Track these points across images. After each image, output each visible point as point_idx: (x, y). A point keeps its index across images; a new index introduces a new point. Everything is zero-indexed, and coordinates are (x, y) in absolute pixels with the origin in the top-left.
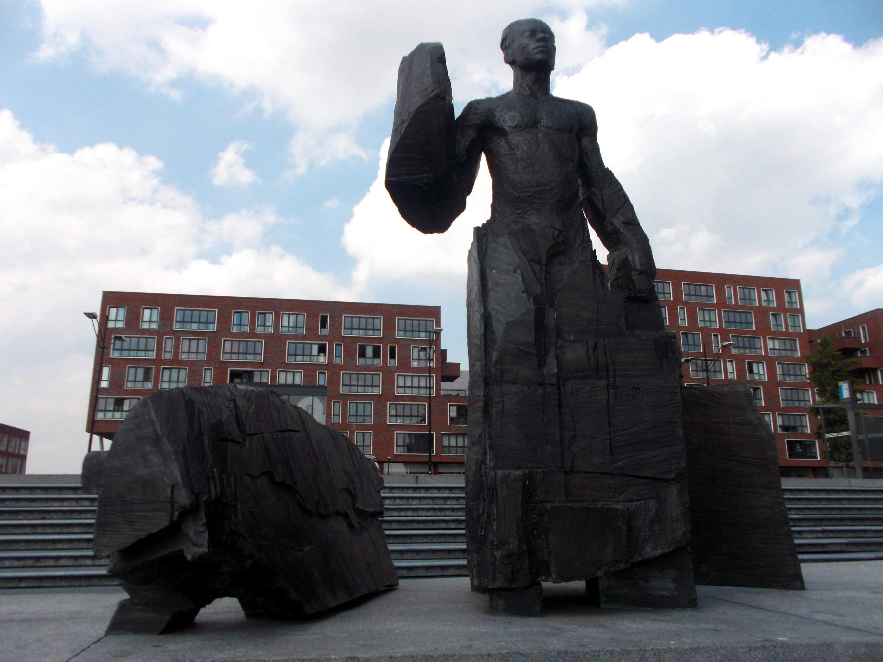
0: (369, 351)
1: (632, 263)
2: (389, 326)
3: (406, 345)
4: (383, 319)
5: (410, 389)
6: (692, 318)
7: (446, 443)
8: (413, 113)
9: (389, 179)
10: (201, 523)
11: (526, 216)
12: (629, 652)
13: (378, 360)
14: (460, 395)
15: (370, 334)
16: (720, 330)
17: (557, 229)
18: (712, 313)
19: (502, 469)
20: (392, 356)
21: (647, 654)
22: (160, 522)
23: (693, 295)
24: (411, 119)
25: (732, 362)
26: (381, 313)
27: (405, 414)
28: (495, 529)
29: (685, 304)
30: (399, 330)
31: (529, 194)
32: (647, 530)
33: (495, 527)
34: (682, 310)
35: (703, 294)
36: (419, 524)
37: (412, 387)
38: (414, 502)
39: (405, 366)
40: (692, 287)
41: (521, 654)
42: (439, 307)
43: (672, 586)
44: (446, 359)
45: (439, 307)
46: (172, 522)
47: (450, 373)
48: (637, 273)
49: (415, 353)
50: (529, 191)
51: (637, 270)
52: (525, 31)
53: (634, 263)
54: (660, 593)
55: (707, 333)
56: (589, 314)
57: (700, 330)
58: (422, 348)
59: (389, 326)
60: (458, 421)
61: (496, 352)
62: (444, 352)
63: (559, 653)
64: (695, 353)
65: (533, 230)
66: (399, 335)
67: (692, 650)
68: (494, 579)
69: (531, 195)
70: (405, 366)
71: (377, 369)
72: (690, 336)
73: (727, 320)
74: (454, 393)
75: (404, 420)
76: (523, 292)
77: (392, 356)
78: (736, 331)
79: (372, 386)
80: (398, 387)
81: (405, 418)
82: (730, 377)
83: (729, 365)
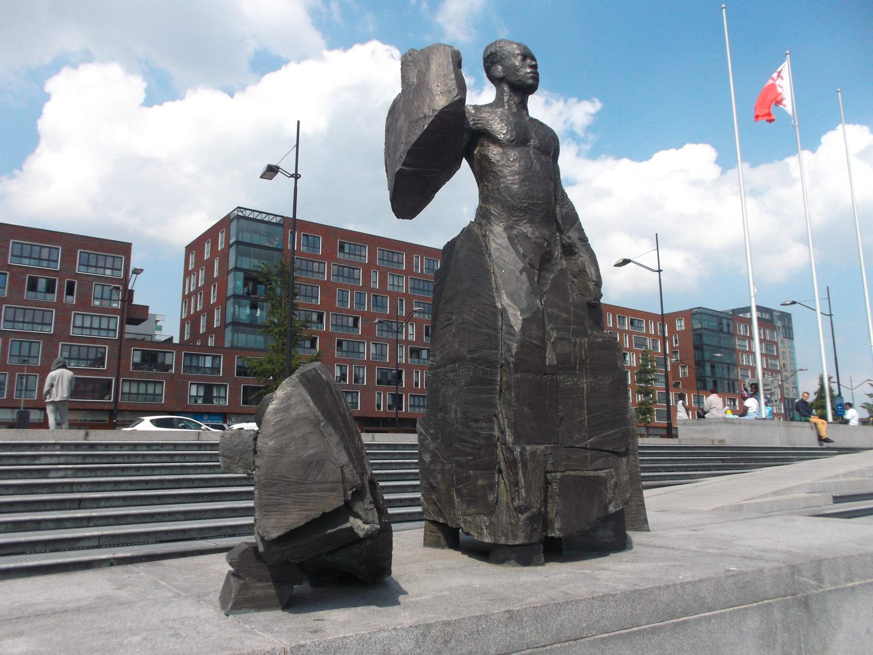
0: (42, 284)
2: (69, 259)
3: (87, 281)
4: (62, 250)
5: (106, 332)
6: (383, 282)
7: (126, 389)
9: (404, 168)
10: (369, 501)
11: (520, 224)
12: (668, 587)
13: (52, 295)
14: (146, 340)
15: (44, 265)
16: (406, 295)
17: (547, 240)
18: (400, 279)
19: (530, 444)
20: (70, 292)
21: (678, 587)
22: (335, 502)
23: (386, 260)
24: (436, 116)
25: (413, 325)
26: (59, 243)
27: (81, 357)
28: (525, 496)
29: (378, 268)
30: (80, 264)
31: (526, 205)
32: (612, 492)
33: (524, 494)
34: (375, 274)
35: (394, 260)
36: (221, 481)
37: (100, 329)
38: (204, 459)
39: (84, 304)
40: (386, 253)
41: (611, 595)
42: (130, 244)
43: (611, 534)
44: (132, 301)
45: (130, 244)
47: (139, 316)
49: (97, 290)
51: (594, 281)
52: (518, 54)
53: (591, 274)
54: (603, 540)
55: (394, 296)
56: (566, 315)
57: (389, 293)
58: (114, 287)
59: (69, 259)
60: (142, 367)
61: (515, 344)
62: (131, 292)
63: (632, 592)
64: (383, 315)
65: (529, 238)
66: (79, 269)
67: (700, 581)
68: (515, 537)
69: (526, 207)
70: (84, 304)
71: (50, 305)
72: (379, 299)
73: (412, 286)
74: (140, 337)
75: (78, 363)
76: (531, 293)
77: (70, 292)
78: (419, 298)
79: (42, 324)
80: (74, 327)
81: (80, 361)
82: (410, 338)
83: (410, 327)
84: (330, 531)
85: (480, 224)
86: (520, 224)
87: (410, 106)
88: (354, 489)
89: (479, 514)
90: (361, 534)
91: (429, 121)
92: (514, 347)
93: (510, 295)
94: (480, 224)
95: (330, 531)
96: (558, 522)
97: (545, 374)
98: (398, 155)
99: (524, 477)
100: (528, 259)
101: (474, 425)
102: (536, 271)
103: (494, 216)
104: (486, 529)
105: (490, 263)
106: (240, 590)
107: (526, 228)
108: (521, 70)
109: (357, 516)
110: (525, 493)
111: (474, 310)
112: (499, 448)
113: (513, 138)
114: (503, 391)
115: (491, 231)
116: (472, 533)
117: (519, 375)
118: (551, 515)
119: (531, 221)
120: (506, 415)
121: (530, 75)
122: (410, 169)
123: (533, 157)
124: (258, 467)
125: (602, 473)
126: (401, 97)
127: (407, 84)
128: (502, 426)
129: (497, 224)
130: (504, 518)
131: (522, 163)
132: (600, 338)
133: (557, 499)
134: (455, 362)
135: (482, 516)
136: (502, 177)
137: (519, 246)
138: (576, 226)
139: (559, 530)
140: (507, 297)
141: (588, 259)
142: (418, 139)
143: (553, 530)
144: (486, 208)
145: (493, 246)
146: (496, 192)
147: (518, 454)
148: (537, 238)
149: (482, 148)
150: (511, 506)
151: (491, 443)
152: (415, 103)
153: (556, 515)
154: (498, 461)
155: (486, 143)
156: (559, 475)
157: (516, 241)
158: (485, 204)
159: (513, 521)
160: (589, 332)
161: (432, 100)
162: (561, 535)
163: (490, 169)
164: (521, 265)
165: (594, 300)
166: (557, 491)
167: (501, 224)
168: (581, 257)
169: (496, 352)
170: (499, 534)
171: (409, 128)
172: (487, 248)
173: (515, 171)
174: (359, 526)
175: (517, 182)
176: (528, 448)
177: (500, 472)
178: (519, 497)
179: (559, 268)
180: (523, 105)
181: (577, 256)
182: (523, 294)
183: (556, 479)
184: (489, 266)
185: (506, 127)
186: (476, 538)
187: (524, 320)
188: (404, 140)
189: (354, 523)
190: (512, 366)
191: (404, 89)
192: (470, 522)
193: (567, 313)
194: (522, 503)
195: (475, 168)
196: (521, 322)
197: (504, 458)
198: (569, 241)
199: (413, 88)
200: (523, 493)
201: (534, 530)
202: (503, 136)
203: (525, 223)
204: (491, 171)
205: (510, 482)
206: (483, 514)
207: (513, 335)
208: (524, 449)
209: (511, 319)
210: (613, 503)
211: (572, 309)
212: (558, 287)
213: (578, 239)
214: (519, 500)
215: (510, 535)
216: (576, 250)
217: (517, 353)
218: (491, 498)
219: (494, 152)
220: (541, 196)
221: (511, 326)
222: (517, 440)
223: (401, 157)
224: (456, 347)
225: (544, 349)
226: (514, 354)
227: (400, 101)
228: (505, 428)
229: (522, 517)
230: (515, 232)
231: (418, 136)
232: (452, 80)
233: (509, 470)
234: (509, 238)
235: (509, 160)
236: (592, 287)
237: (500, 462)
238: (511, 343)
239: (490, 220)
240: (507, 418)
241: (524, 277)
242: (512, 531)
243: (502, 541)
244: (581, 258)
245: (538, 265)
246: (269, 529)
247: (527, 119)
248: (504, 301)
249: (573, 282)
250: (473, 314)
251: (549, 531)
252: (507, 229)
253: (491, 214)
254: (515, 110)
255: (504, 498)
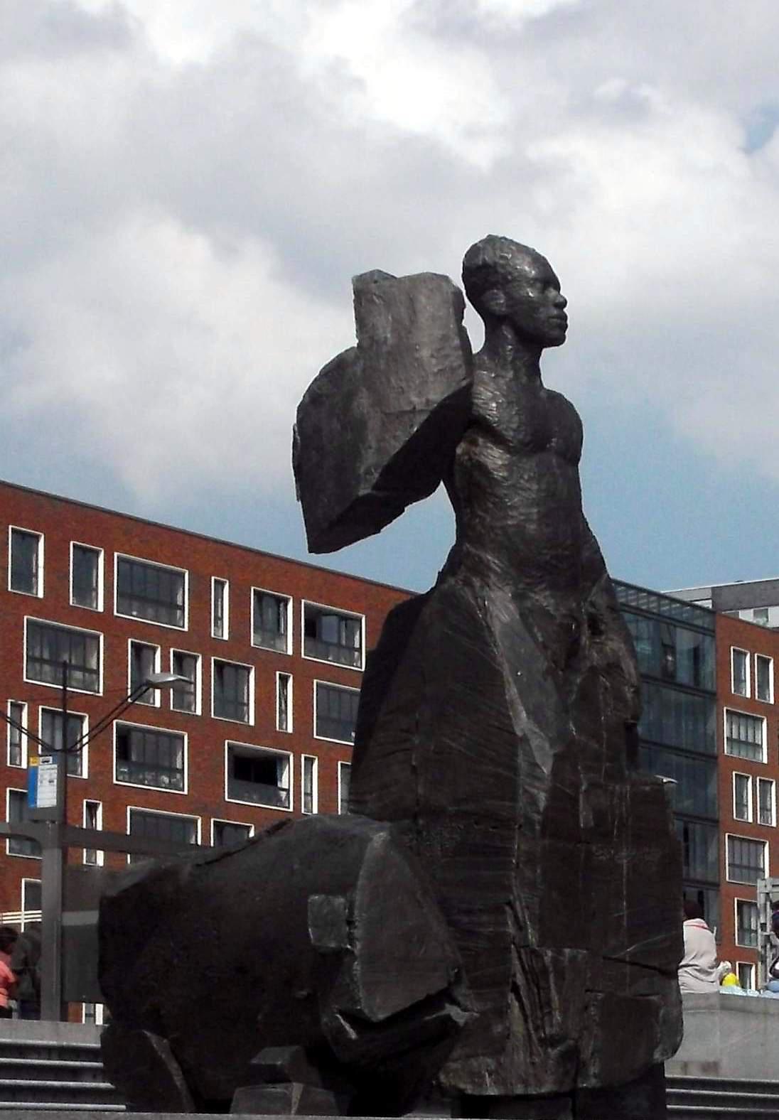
1: (626, 671)
8: (435, 405)
17: (575, 619)
22: (437, 984)
24: (434, 413)
28: (560, 1021)
33: (559, 1018)
46: (450, 984)
48: (632, 690)
50: (547, 554)
65: (552, 617)
68: (540, 1083)
84: (428, 1018)
85: (468, 583)
86: (536, 590)
87: (381, 383)
88: (456, 971)
89: (476, 1055)
90: (461, 1022)
91: (422, 418)
92: (542, 798)
93: (534, 714)
94: (468, 583)
95: (428, 1018)
96: (597, 1064)
97: (580, 842)
98: (362, 471)
99: (559, 992)
100: (549, 652)
101: (465, 919)
102: (560, 673)
103: (496, 573)
104: (490, 1075)
105: (500, 659)
106: (302, 1095)
107: (543, 599)
108: (541, 310)
109: (454, 1002)
110: (560, 1016)
111: (467, 734)
112: (514, 955)
113: (528, 438)
114: (521, 865)
115: (490, 599)
116: (462, 1086)
117: (547, 842)
118: (586, 1054)
119: (553, 587)
120: (526, 901)
121: (555, 320)
122: (380, 494)
123: (558, 472)
124: (357, 939)
125: (654, 998)
126: (357, 358)
127: (372, 338)
128: (521, 919)
129: (500, 588)
130: (520, 1057)
131: (544, 486)
132: (646, 784)
133: (596, 1030)
134: (415, 817)
135: (481, 1058)
136: (512, 508)
137: (536, 630)
138: (603, 581)
139: (595, 1076)
140: (528, 717)
141: (622, 645)
142: (401, 450)
143: (586, 1077)
144: (480, 558)
145: (497, 628)
146: (499, 532)
147: (549, 960)
148: (564, 616)
149: (474, 449)
150: (534, 1037)
151: (500, 946)
152: (393, 380)
153: (592, 1054)
154: (512, 973)
155: (481, 441)
156: (600, 996)
157: (531, 620)
158: (477, 549)
159: (537, 1060)
160: (627, 773)
161: (424, 382)
162: (599, 1085)
163: (489, 490)
164: (542, 664)
165: (632, 719)
166: (597, 1018)
167: (507, 589)
168: (612, 640)
169: (510, 804)
170: (514, 1082)
171: (383, 424)
172: (491, 633)
173: (533, 499)
174: (458, 1014)
175: (535, 517)
176: (567, 951)
177: (515, 989)
178: (551, 1022)
179: (588, 664)
180: (535, 371)
181: (603, 637)
182: (550, 714)
183: (597, 1000)
184: (499, 665)
185: (516, 419)
186: (469, 1092)
187: (555, 755)
188: (374, 444)
189: (453, 1011)
190: (538, 827)
191: (365, 344)
192: (456, 1071)
193: (598, 742)
194: (555, 1030)
195: (457, 477)
196: (550, 762)
197: (523, 968)
198: (592, 610)
199: (385, 349)
200: (558, 1017)
201: (566, 1073)
202: (511, 433)
203: (542, 590)
204: (491, 494)
205: (532, 1004)
206: (484, 1055)
207: (539, 779)
208: (560, 953)
209: (536, 754)
210: (660, 1047)
211: (605, 735)
212: (586, 697)
213: (608, 607)
214: (552, 1026)
215: (532, 1080)
216: (603, 627)
217: (546, 808)
218: (498, 1029)
219: (495, 458)
220: (569, 542)
221: (536, 765)
222: (541, 944)
223: (368, 472)
224: (420, 791)
225: (577, 801)
226: (541, 809)
227: (354, 363)
228: (526, 923)
229: (553, 1052)
230: (528, 604)
231: (402, 443)
232: (455, 349)
233: (532, 985)
234: (521, 615)
235: (522, 477)
236: (629, 696)
237: (514, 975)
238: (535, 791)
239: (486, 579)
240: (528, 908)
241: (549, 685)
242: (535, 1075)
243: (519, 1090)
244: (610, 643)
245: (563, 662)
246: (375, 1009)
247: (542, 394)
248: (522, 722)
249: (606, 688)
250: (463, 739)
251: (579, 1080)
252: (518, 597)
253: (490, 569)
254: (524, 380)
255: (518, 1027)
